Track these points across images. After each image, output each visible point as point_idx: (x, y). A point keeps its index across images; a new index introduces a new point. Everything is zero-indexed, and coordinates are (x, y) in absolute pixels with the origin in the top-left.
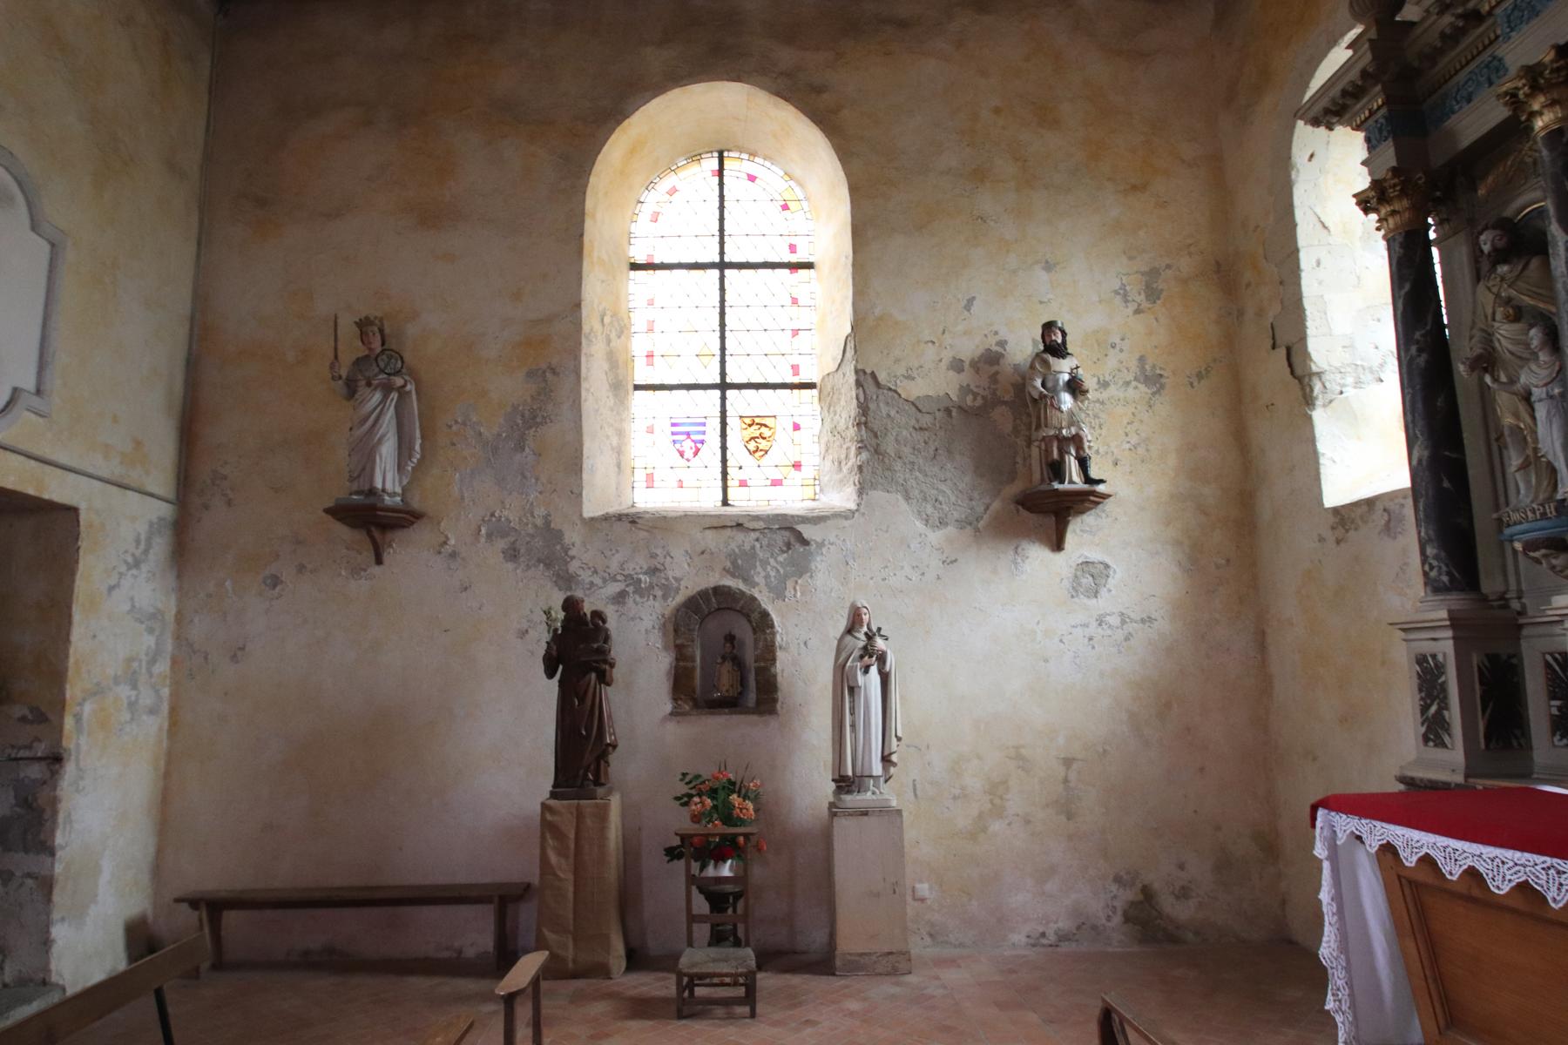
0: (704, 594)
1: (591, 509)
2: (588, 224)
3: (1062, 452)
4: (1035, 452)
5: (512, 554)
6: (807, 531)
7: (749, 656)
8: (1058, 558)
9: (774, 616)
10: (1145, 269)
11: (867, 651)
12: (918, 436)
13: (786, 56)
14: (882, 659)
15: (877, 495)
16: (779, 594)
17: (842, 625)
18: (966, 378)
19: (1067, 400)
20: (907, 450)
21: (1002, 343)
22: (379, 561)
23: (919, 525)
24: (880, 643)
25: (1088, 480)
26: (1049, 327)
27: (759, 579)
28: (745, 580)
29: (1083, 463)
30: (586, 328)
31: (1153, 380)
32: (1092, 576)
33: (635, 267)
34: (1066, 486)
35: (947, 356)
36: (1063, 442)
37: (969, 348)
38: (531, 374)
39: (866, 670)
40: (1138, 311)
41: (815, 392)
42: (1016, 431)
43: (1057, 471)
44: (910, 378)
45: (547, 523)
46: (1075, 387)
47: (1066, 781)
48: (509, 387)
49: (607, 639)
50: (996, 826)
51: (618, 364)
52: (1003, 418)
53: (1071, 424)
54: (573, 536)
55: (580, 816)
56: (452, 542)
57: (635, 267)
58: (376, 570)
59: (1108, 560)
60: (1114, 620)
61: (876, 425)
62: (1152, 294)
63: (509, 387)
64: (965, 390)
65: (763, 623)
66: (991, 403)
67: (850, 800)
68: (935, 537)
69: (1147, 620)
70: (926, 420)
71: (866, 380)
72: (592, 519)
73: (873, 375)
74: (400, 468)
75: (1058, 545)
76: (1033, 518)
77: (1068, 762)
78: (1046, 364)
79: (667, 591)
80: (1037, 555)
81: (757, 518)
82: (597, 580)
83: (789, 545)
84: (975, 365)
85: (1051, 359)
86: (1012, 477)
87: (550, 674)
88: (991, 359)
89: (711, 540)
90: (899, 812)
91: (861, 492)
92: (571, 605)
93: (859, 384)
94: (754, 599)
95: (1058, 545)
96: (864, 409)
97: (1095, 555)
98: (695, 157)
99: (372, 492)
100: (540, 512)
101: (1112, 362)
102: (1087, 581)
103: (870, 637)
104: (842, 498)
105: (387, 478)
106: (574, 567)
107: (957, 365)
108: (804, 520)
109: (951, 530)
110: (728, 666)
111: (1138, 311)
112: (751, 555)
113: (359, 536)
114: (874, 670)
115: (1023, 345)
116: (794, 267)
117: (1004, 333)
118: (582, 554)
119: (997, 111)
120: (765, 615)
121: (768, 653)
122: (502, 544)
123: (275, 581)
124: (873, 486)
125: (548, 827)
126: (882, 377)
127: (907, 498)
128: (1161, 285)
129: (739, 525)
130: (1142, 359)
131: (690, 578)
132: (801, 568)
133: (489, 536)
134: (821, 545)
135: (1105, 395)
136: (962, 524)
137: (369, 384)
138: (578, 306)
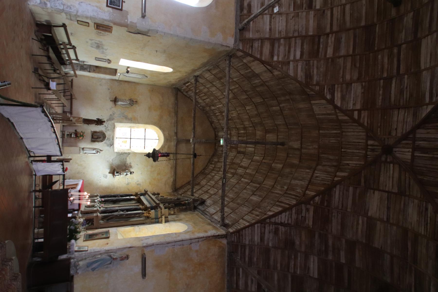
0: (105, 135)
1: (116, 124)
2: (148, 125)
3: (120, 173)
4: (120, 171)
5: (111, 115)
6: (112, 146)
7: (98, 140)
8: (108, 173)
9: (102, 143)
10: (141, 184)
11: (98, 152)
12: (123, 159)
13: (166, 147)
14: (97, 153)
15: (116, 154)
16: (105, 143)
17: (101, 149)
18: (129, 164)
19: (125, 174)
20: (121, 157)
21: (133, 168)
22: (111, 101)
23: (112, 158)
24: (99, 153)
25: (116, 176)
26: (133, 172)
27: (107, 141)
28: (107, 140)
29: (118, 175)
30: (136, 124)
31: (128, 184)
32: (106, 177)
33: (145, 129)
34: (115, 173)
35: (131, 162)
36: (120, 173)
37: (132, 165)
38: (131, 118)
39: (96, 151)
40: (136, 183)
41: (129, 148)
42: (123, 169)
43: (117, 173)
44: (129, 158)
45: (114, 119)
46: (127, 174)
47: (82, 173)
48: (130, 116)
49: (100, 125)
50: (77, 165)
51: (133, 127)
52: (124, 168)
53: (123, 174)
54: (113, 122)
55: (81, 121)
56: (113, 109)
57: (145, 129)
58: (110, 100)
59: (107, 178)
60: (100, 179)
61: (124, 154)
62: (138, 184)
63: (130, 116)
64: (127, 164)
65: (102, 141)
66: (126, 167)
67: (81, 149)
68: (111, 160)
69: (100, 182)
70: (124, 160)
71: (129, 154)
72: (114, 124)
73: (129, 154)
74: (121, 104)
75: (109, 173)
76: (112, 171)
77: (84, 173)
78: (129, 172)
79: (106, 131)
80: (108, 171)
81: (114, 141)
82: (107, 124)
83: (110, 144)
84: (130, 165)
85: (130, 172)
86: (118, 169)
87: (97, 119)
88: (131, 167)
89: (112, 136)
90: (80, 154)
91: (116, 152)
92: (104, 122)
93: (129, 153)
94: (104, 140)
95: (109, 173)
96: (126, 153)
97: (108, 177)
98: (158, 136)
99: (118, 101)
100: (116, 118)
101: (130, 180)
102: (105, 176)
103: (99, 152)
104: (116, 150)
105: (120, 103)
106: (109, 121)
107: (130, 163)
108: (113, 146)
109: (111, 162)
110: (97, 137)
111: (136, 183)
112: (109, 140)
113: (113, 99)
114: (96, 152)
115: (132, 170)
116: (144, 147)
117: (134, 168)
118: (110, 122)
119: (159, 169)
120: (103, 141)
121: (98, 142)
122: (112, 114)
123: (109, 89)
124: (117, 154)
125: (80, 118)
126: (129, 155)
127: (115, 157)
128: (139, 185)
129: (113, 139)
130: (130, 183)
131: (107, 134)
132: (108, 145)
133: (113, 113)
134: (110, 148)
135: (126, 179)
136: (112, 163)
137: (130, 102)
138: (139, 123)
